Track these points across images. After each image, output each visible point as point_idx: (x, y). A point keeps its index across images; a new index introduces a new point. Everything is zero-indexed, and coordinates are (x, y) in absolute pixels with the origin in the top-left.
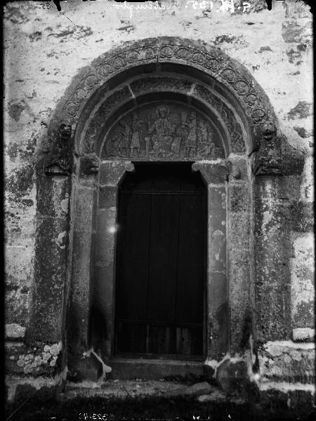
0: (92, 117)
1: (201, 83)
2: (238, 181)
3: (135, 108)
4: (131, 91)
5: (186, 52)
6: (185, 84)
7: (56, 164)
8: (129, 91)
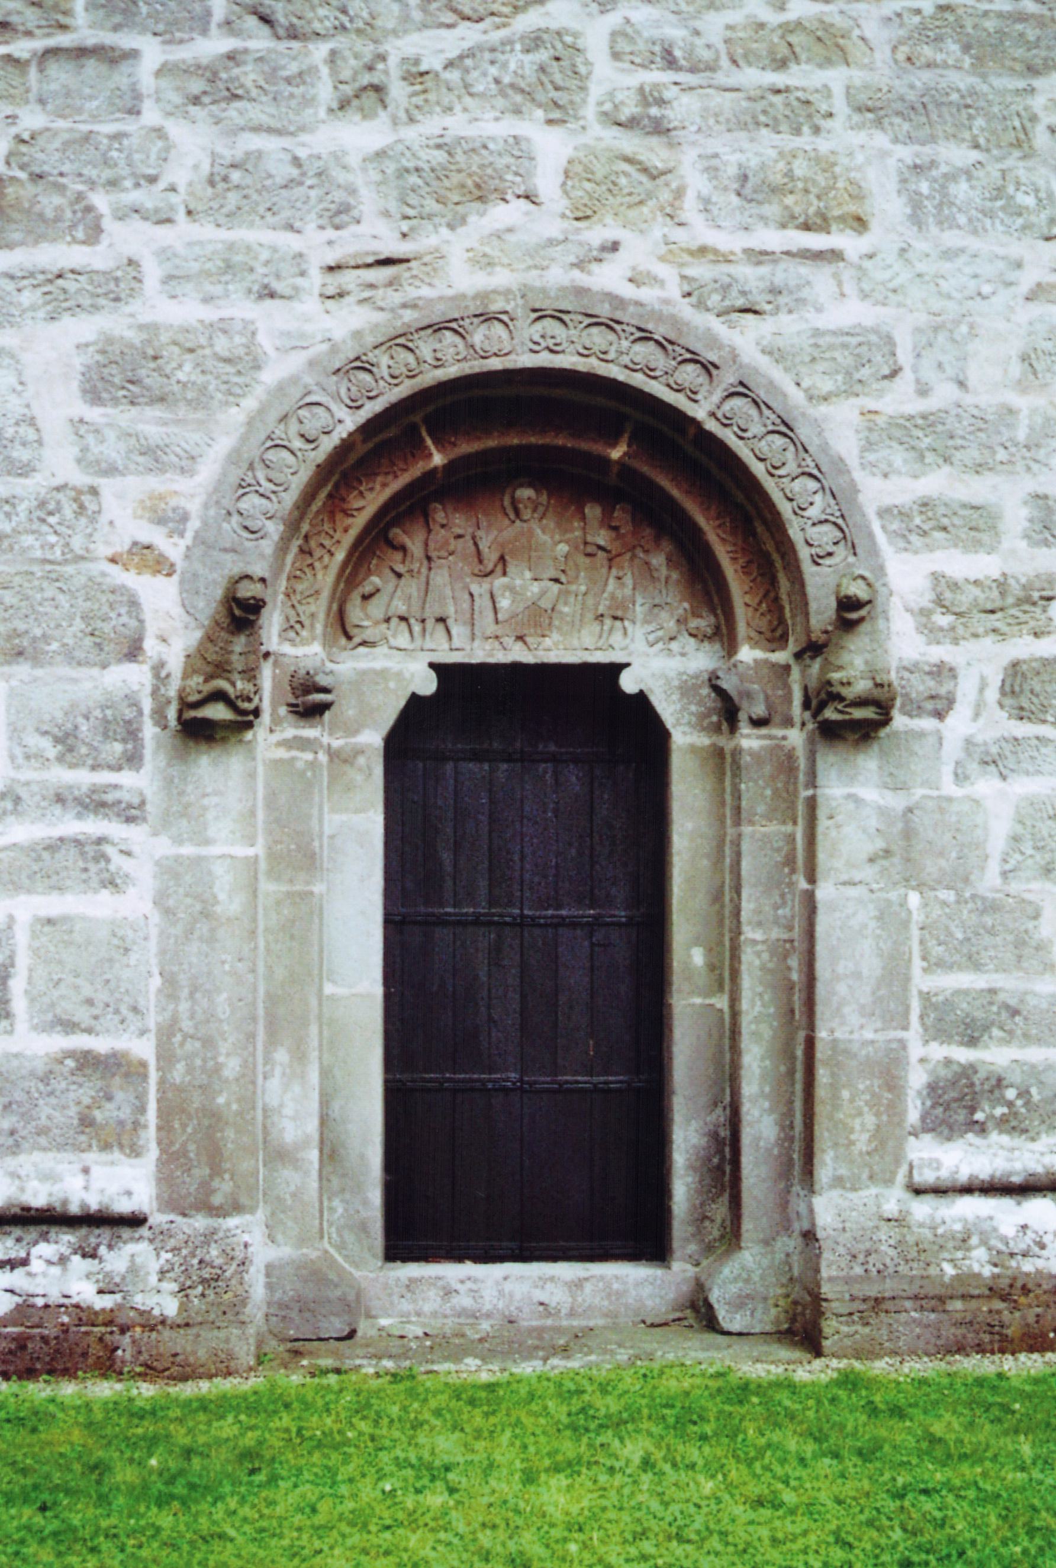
2: (764, 731)
4: (429, 442)
5: (612, 336)
7: (218, 696)
8: (423, 441)
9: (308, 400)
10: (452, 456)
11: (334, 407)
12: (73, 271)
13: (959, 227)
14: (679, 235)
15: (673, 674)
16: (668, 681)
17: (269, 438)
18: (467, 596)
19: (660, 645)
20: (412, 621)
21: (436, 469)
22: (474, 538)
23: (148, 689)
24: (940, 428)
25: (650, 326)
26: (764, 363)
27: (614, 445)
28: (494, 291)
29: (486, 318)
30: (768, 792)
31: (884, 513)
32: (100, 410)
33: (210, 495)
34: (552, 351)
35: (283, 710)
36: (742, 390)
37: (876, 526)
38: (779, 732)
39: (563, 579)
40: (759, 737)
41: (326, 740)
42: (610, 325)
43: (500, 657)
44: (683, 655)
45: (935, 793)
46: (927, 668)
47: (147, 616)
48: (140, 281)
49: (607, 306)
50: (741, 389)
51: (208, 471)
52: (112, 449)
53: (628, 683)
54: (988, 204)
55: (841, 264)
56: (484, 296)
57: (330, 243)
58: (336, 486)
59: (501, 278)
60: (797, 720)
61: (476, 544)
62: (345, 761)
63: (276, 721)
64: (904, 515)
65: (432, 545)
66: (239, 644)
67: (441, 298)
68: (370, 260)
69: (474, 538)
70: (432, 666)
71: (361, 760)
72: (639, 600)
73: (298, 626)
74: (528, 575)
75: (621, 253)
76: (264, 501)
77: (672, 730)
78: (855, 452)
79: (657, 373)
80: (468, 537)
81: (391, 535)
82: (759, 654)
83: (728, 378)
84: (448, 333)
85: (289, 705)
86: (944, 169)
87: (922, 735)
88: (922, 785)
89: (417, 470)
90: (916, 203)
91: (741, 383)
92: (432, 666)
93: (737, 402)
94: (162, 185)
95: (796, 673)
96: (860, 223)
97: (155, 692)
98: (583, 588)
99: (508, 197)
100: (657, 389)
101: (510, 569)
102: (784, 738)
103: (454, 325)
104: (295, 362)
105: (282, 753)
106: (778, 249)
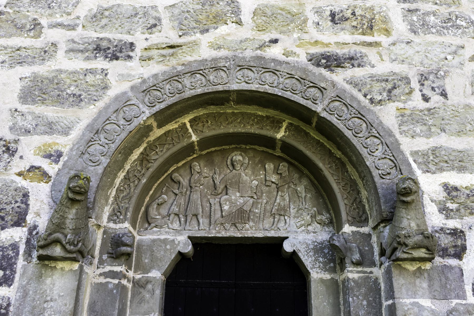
0: (127, 167)
1: (296, 122)
3: (195, 156)
4: (190, 130)
6: (273, 122)
8: (188, 130)
9: (128, 103)
10: (201, 137)
11: (141, 106)
12: (25, 48)
13: (433, 33)
14: (306, 37)
15: (310, 242)
16: (308, 245)
17: (108, 119)
18: (208, 205)
19: (303, 228)
20: (181, 216)
21: (193, 142)
22: (213, 178)
23: (24, 241)
24: (436, 116)
25: (293, 73)
26: (348, 87)
27: (278, 132)
28: (220, 58)
29: (217, 69)
30: (365, 303)
31: (414, 153)
32: (27, 106)
33: (74, 145)
34: (247, 83)
35: (105, 257)
36: (338, 98)
37: (411, 160)
38: (368, 270)
39: (255, 197)
40: (358, 272)
41: (131, 274)
42: (274, 72)
43: (223, 234)
44: (315, 232)
45: (464, 302)
46: (448, 231)
47: (32, 201)
48: (56, 52)
49: (273, 64)
50: (338, 99)
51: (75, 134)
52: (28, 123)
53: (287, 247)
54: (445, 25)
55: (381, 48)
56: (215, 60)
57: (146, 39)
58: (145, 149)
59: (223, 53)
60: (378, 263)
61: (214, 181)
62: (142, 287)
63: (101, 262)
64: (425, 155)
65: (192, 181)
66: (72, 213)
67: (195, 61)
68: (164, 46)
69: (213, 178)
70: (190, 238)
71: (150, 286)
72: (292, 207)
73: (119, 214)
74: (238, 194)
75: (279, 43)
76: (101, 148)
77: (310, 271)
78: (397, 126)
79: (297, 92)
80: (210, 178)
81: (173, 177)
82: (354, 229)
83: (330, 94)
84: (198, 75)
85: (108, 253)
86: (422, 11)
87: (450, 268)
88: (455, 298)
89: (185, 143)
90: (412, 24)
91: (337, 96)
92: (190, 238)
93: (337, 104)
94: (73, 17)
95: (374, 239)
96: (387, 32)
97: (28, 242)
98: (265, 201)
99: (228, 22)
100: (297, 98)
101: (230, 191)
102: (371, 272)
103: (201, 72)
104: (125, 86)
105: (102, 280)
106: (351, 42)
